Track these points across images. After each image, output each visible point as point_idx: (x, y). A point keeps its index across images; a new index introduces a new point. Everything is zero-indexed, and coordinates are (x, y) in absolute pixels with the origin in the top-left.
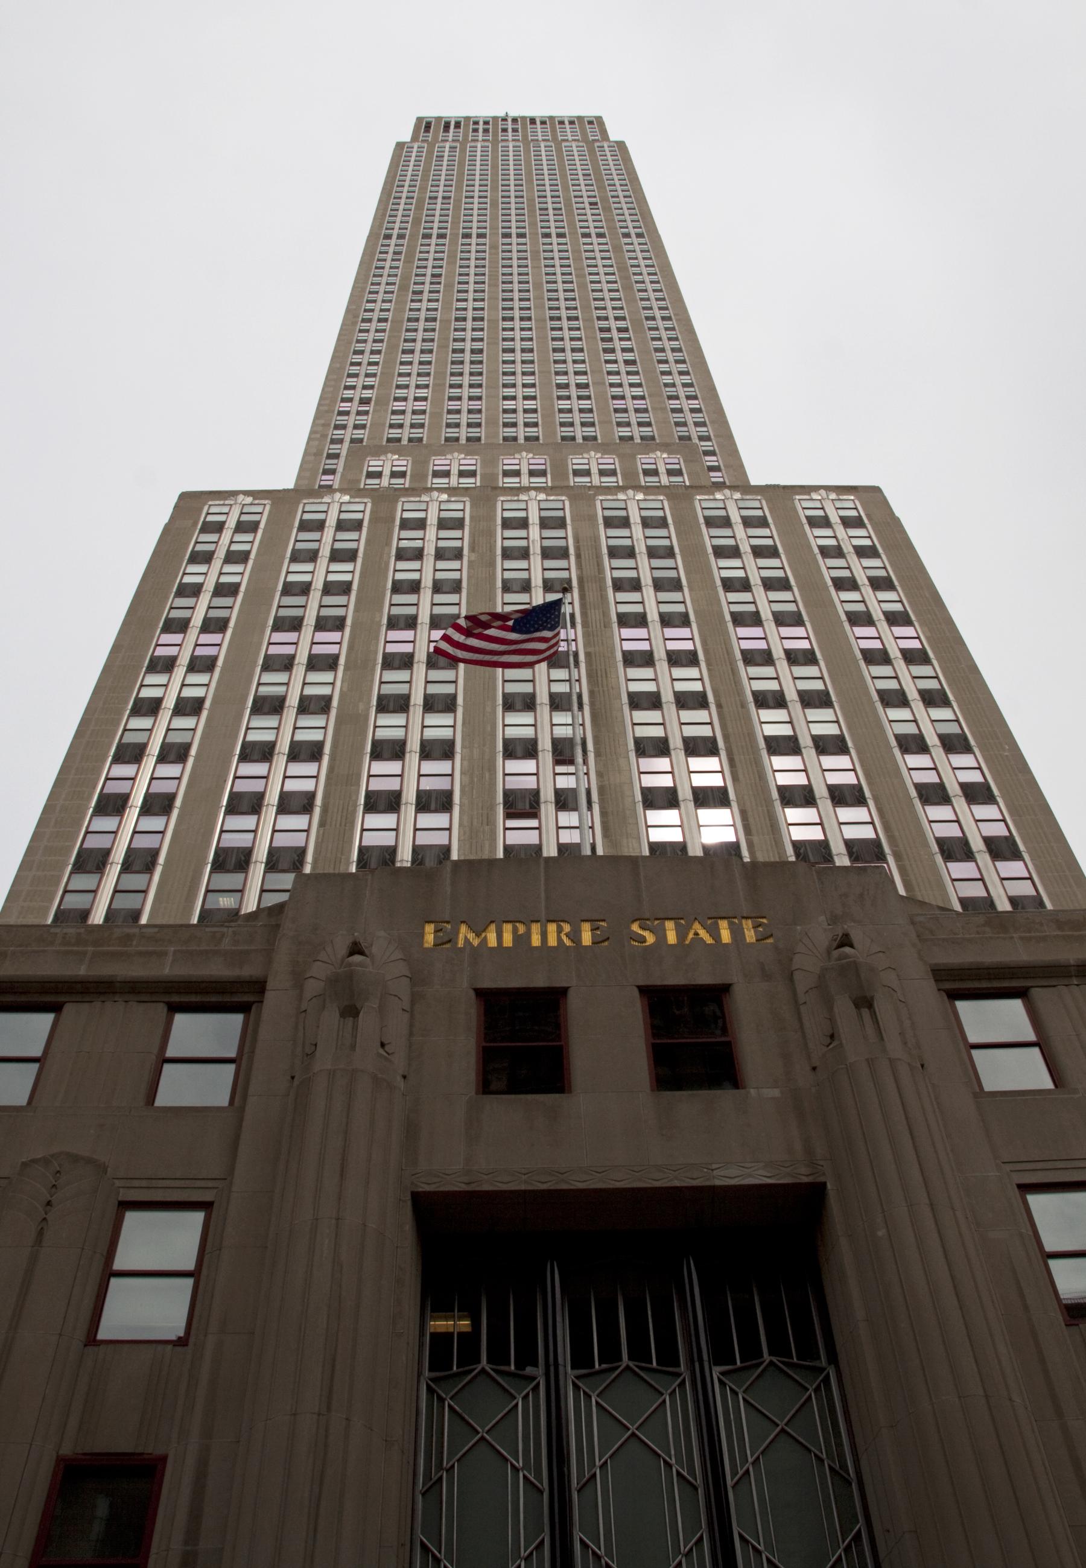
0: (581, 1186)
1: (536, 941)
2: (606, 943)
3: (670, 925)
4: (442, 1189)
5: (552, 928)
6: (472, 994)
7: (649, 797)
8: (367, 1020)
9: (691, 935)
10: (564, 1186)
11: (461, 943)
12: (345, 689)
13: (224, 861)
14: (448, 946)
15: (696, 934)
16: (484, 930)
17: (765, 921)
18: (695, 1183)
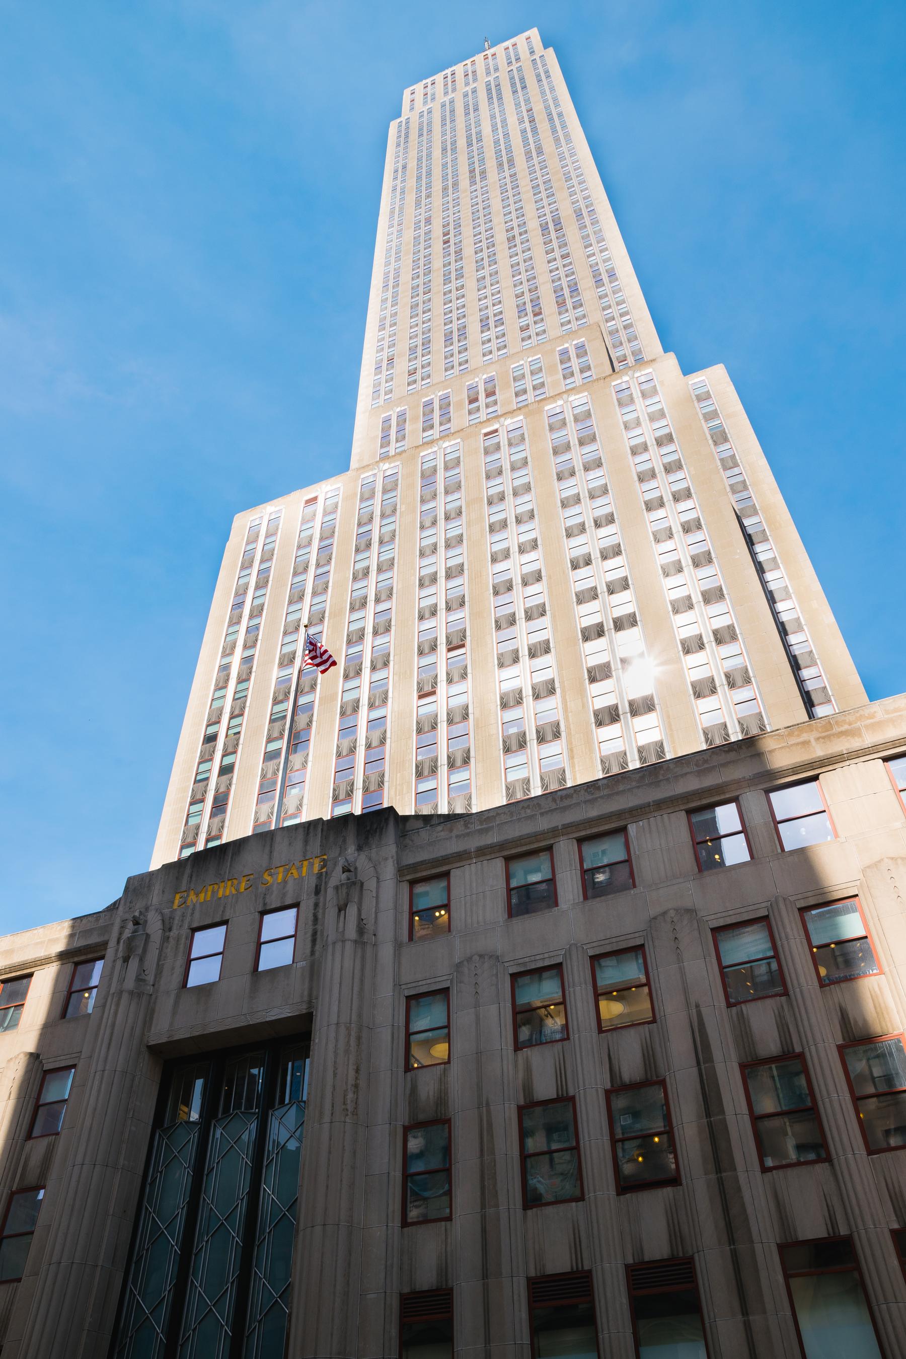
0: (212, 1030)
1: (220, 894)
2: (250, 889)
3: (281, 869)
4: (160, 1042)
5: (229, 883)
6: (190, 932)
7: (502, 660)
8: (134, 964)
9: (289, 875)
10: (205, 1033)
11: (189, 903)
12: (329, 633)
13: (266, 772)
14: (183, 906)
15: (292, 873)
16: (201, 893)
17: (325, 857)
18: (258, 1021)
